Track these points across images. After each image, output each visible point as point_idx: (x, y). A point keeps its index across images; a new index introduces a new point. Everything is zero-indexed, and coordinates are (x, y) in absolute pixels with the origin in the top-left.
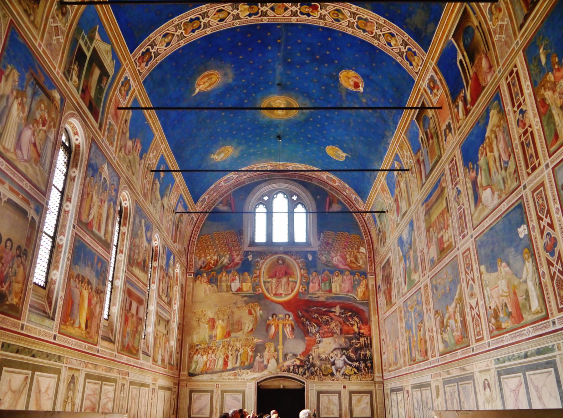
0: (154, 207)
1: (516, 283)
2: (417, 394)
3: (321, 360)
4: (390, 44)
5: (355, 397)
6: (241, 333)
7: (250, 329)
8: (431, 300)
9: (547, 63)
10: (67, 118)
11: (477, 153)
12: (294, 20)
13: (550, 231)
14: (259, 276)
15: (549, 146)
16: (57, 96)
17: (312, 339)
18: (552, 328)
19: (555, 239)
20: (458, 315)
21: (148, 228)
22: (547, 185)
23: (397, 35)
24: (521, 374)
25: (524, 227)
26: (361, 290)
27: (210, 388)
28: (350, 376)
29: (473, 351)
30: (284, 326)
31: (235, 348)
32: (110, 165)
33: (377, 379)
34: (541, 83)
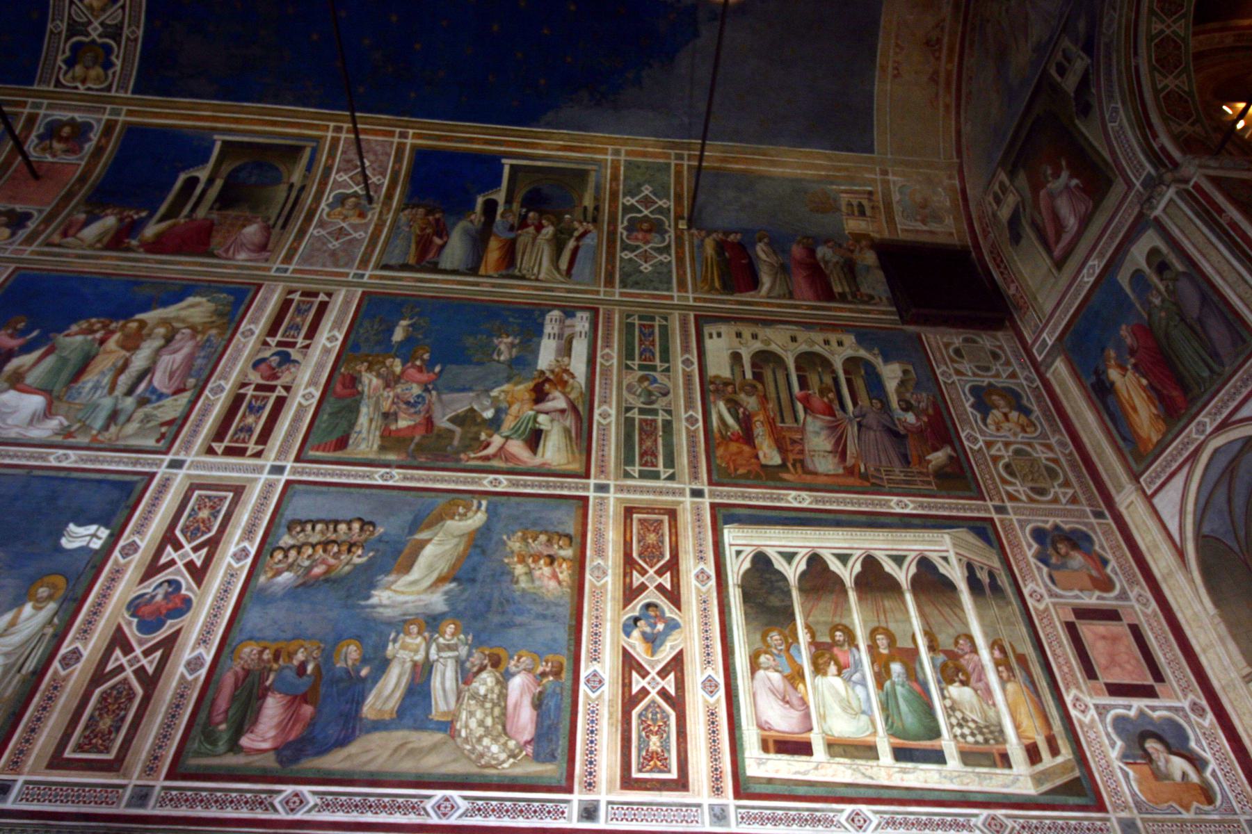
9: (401, 343)
11: (75, 320)
13: (186, 580)
15: (308, 445)
23: (123, 7)
34: (367, 356)
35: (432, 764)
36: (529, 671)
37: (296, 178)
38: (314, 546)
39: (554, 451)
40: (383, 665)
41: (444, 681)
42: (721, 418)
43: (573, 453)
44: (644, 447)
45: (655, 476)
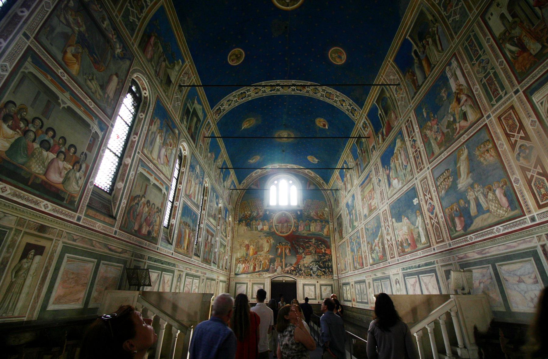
0: (220, 187)
1: (412, 228)
2: (358, 286)
3: (305, 267)
4: (342, 105)
5: (323, 288)
6: (263, 252)
7: (267, 250)
8: (365, 236)
10: (181, 142)
12: (293, 93)
13: (431, 201)
14: (272, 223)
16: (177, 132)
17: (300, 256)
18: (433, 252)
19: (434, 205)
20: (380, 244)
21: (217, 197)
22: (429, 178)
24: (417, 276)
25: (416, 199)
26: (325, 230)
27: (246, 282)
28: (320, 276)
29: (389, 263)
30: (285, 249)
31: (259, 260)
32: (200, 165)
33: (335, 278)
35: (491, 221)
36: (499, 187)
37: (388, 95)
38: (443, 182)
39: (472, 116)
40: (468, 202)
41: (482, 200)
42: (511, 51)
43: (476, 112)
44: (492, 90)
45: (501, 98)
